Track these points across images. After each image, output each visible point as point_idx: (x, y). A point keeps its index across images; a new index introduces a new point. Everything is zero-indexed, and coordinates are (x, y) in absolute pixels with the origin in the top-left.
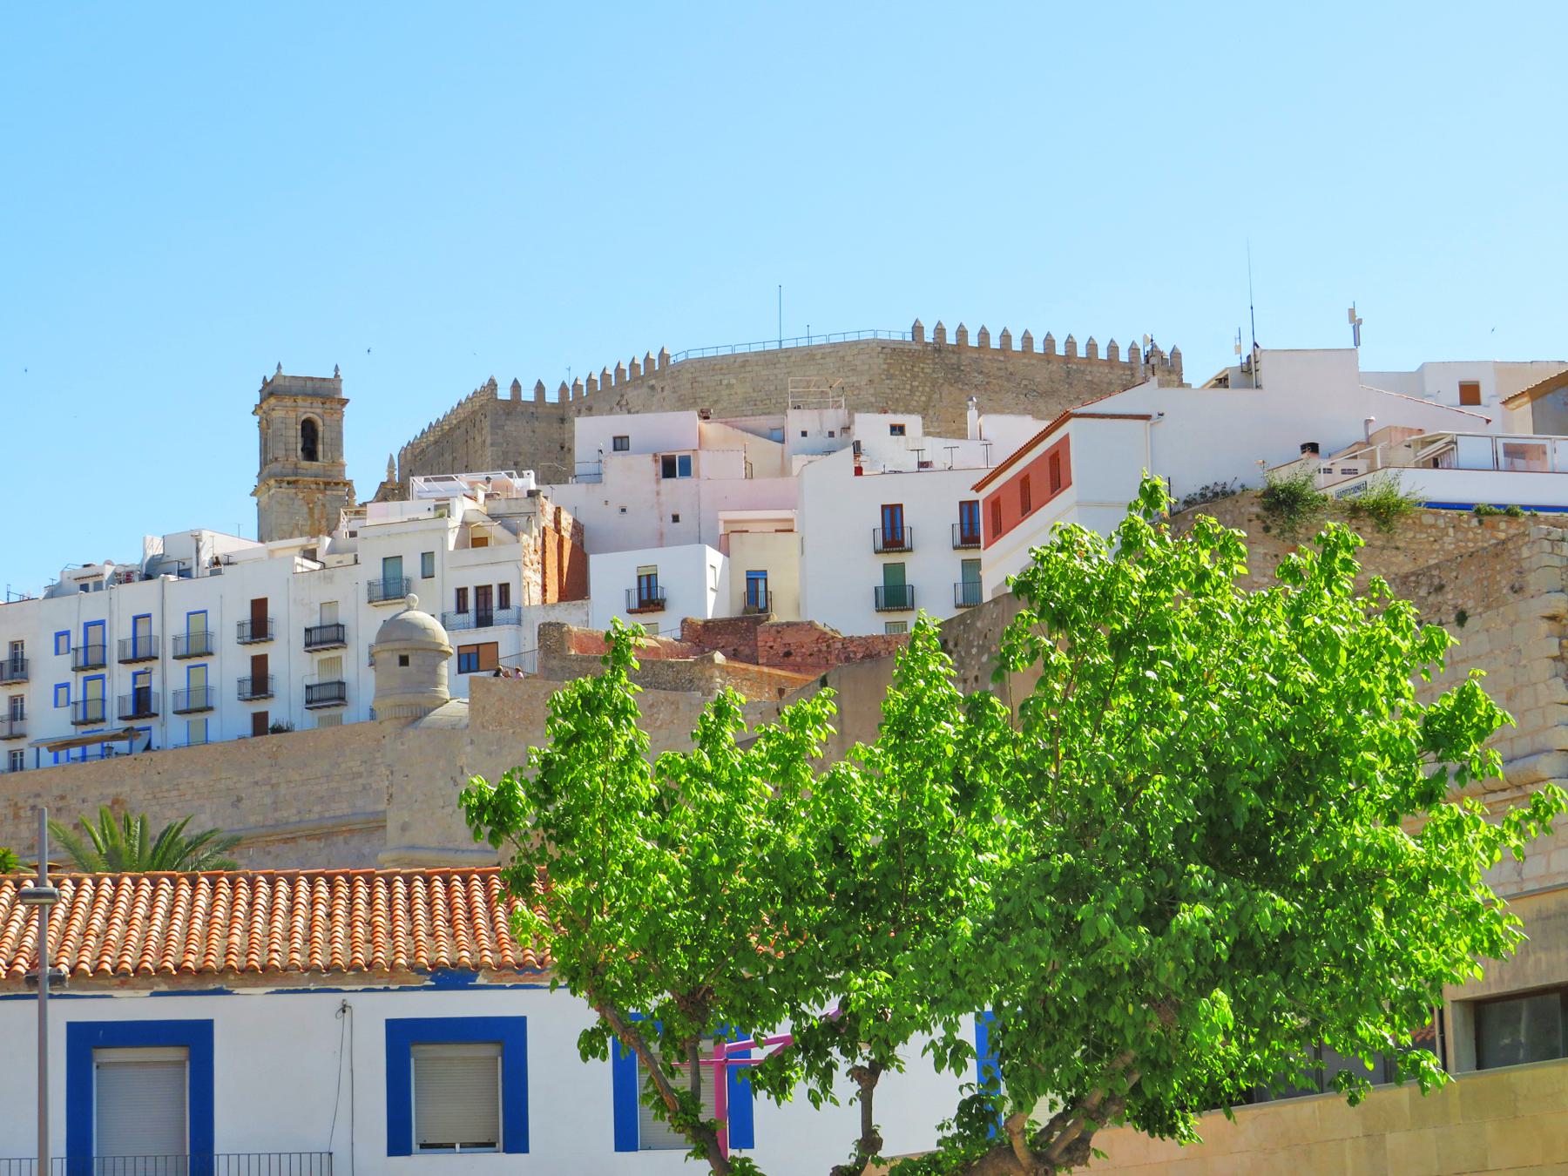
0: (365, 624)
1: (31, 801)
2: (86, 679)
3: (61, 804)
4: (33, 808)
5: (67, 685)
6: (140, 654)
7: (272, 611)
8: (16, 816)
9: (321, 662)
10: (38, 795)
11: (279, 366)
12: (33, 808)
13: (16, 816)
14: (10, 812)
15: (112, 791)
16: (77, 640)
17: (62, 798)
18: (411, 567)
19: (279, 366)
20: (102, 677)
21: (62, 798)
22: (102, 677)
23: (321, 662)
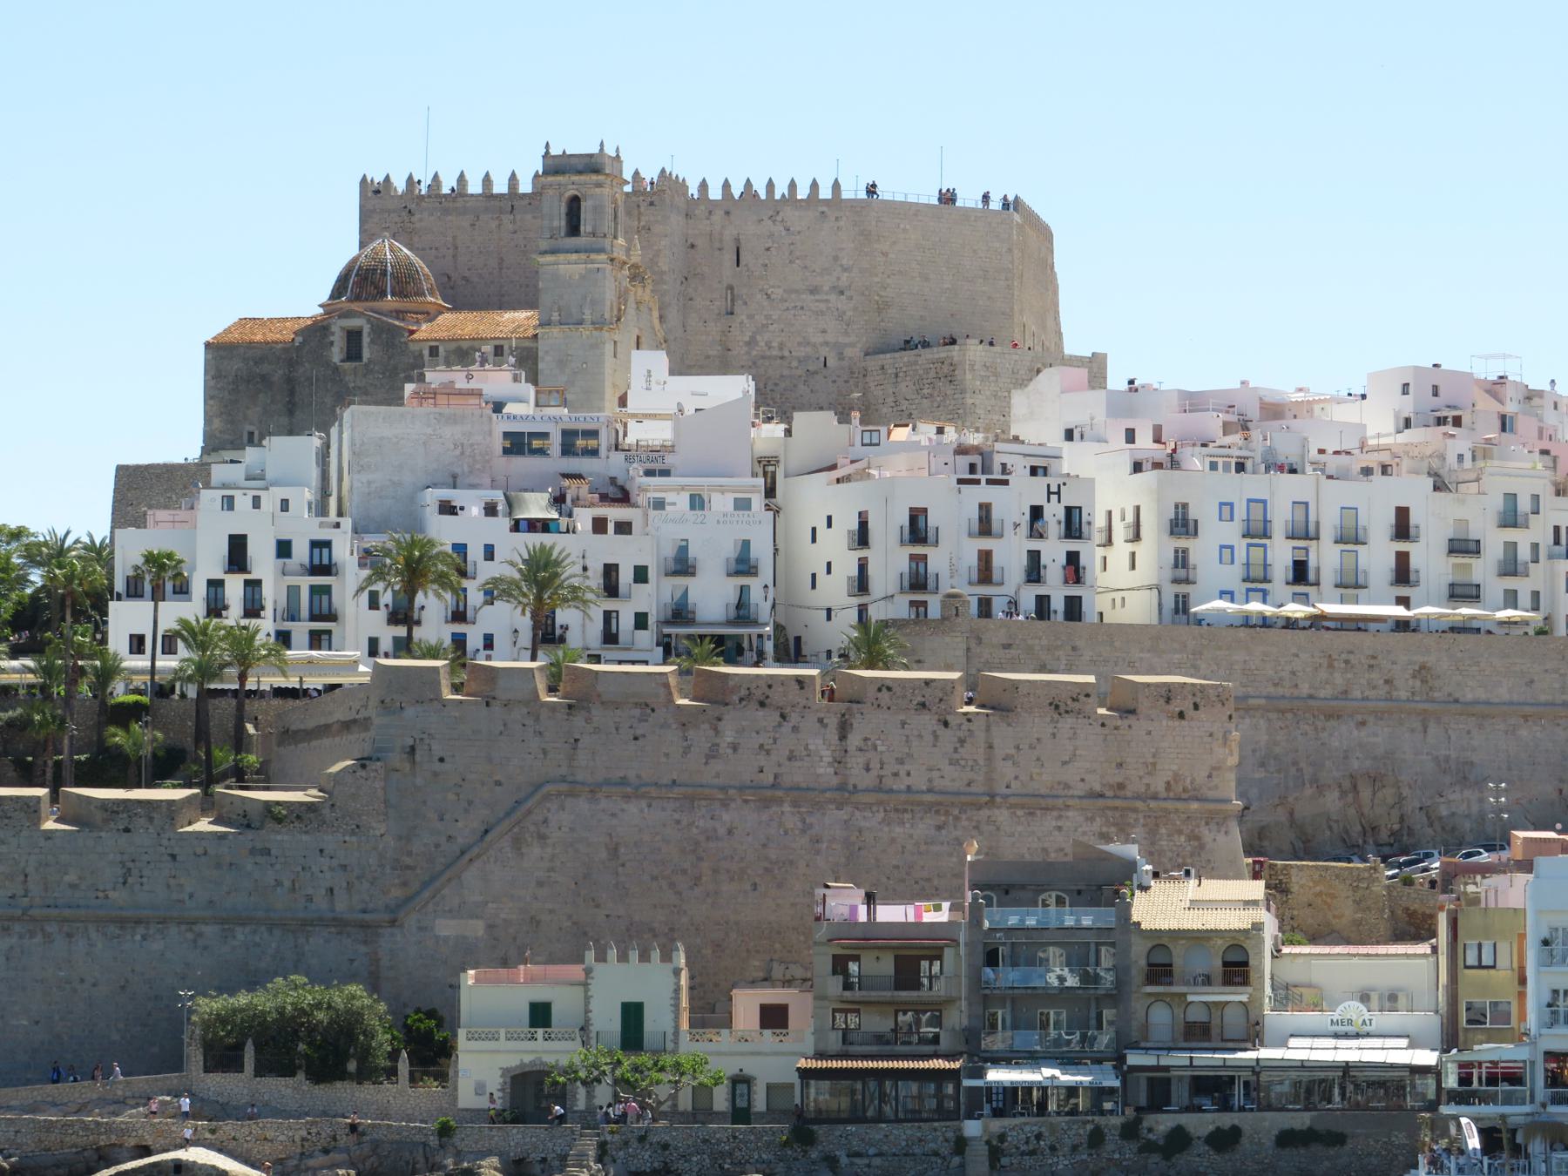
0: (1494, 541)
1: (1344, 656)
2: (1249, 545)
3: (1372, 662)
4: (1347, 662)
5: (1232, 548)
6: (1304, 533)
7: (1414, 519)
8: (1331, 666)
9: (1455, 565)
10: (1351, 652)
11: (602, 144)
12: (1347, 662)
13: (1331, 666)
14: (1325, 662)
15: (1420, 659)
16: (1240, 512)
17: (1374, 657)
18: (1524, 505)
19: (602, 144)
20: (1264, 546)
21: (1374, 657)
22: (1264, 546)
23: (1455, 565)
